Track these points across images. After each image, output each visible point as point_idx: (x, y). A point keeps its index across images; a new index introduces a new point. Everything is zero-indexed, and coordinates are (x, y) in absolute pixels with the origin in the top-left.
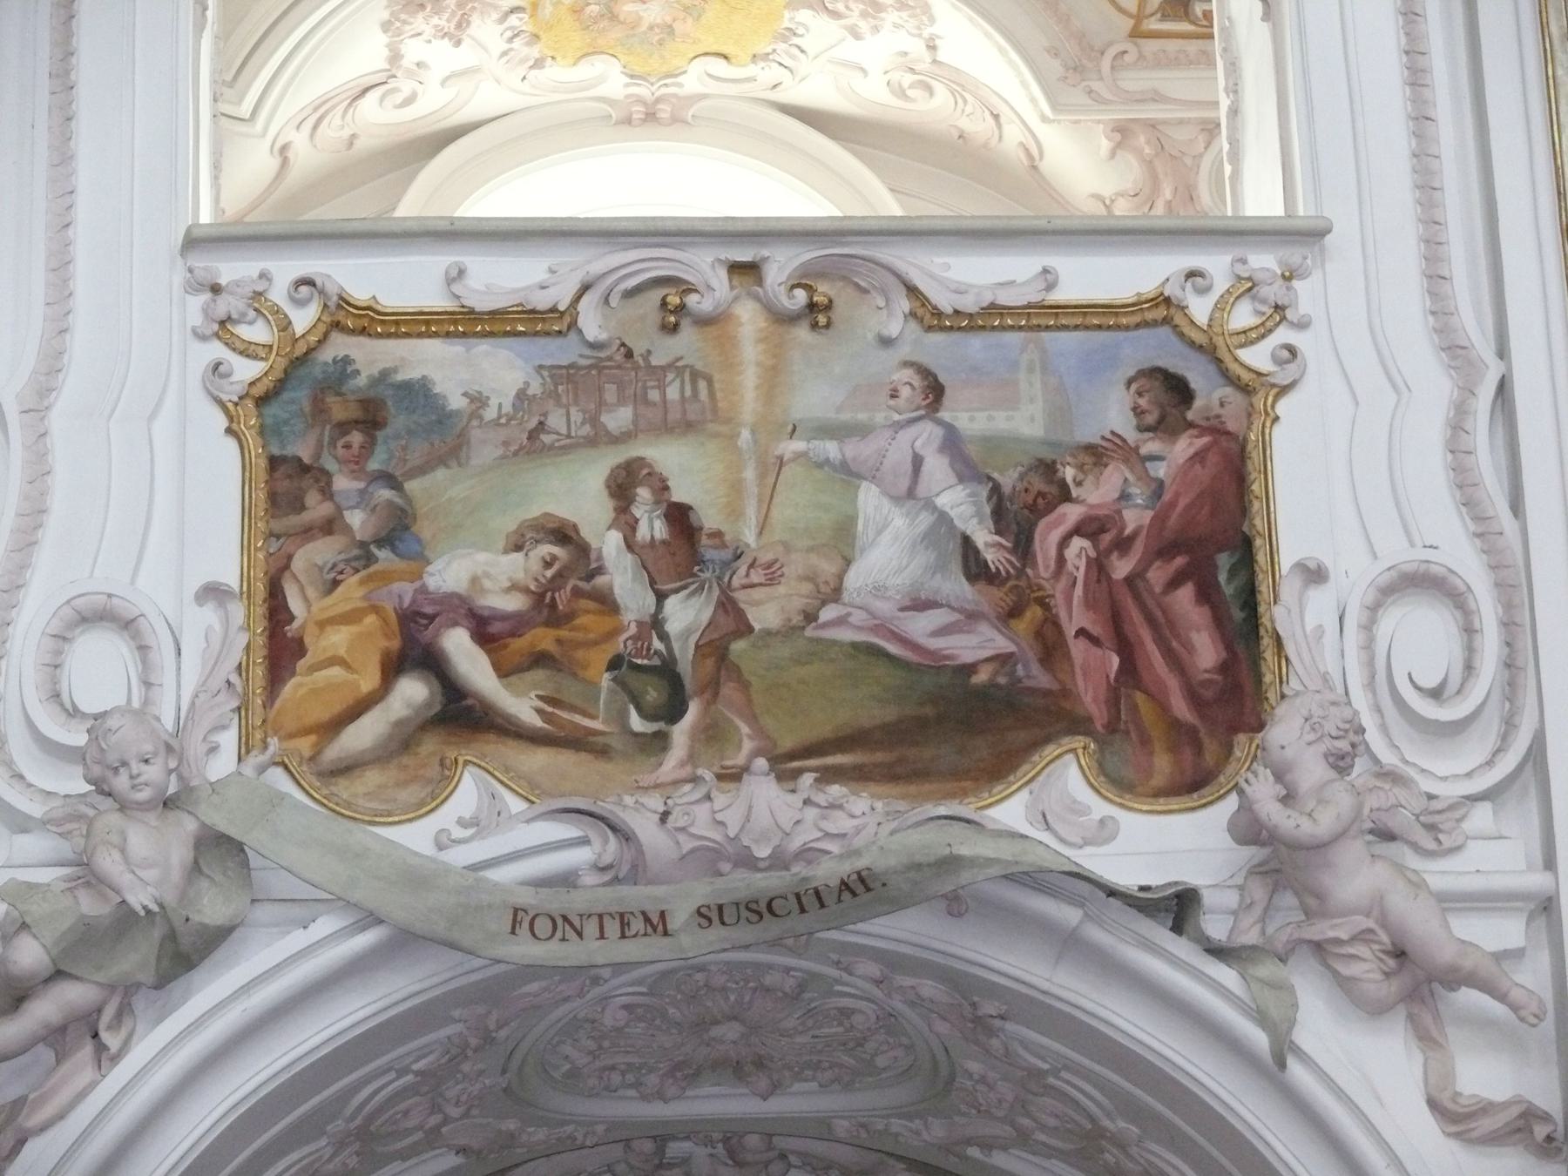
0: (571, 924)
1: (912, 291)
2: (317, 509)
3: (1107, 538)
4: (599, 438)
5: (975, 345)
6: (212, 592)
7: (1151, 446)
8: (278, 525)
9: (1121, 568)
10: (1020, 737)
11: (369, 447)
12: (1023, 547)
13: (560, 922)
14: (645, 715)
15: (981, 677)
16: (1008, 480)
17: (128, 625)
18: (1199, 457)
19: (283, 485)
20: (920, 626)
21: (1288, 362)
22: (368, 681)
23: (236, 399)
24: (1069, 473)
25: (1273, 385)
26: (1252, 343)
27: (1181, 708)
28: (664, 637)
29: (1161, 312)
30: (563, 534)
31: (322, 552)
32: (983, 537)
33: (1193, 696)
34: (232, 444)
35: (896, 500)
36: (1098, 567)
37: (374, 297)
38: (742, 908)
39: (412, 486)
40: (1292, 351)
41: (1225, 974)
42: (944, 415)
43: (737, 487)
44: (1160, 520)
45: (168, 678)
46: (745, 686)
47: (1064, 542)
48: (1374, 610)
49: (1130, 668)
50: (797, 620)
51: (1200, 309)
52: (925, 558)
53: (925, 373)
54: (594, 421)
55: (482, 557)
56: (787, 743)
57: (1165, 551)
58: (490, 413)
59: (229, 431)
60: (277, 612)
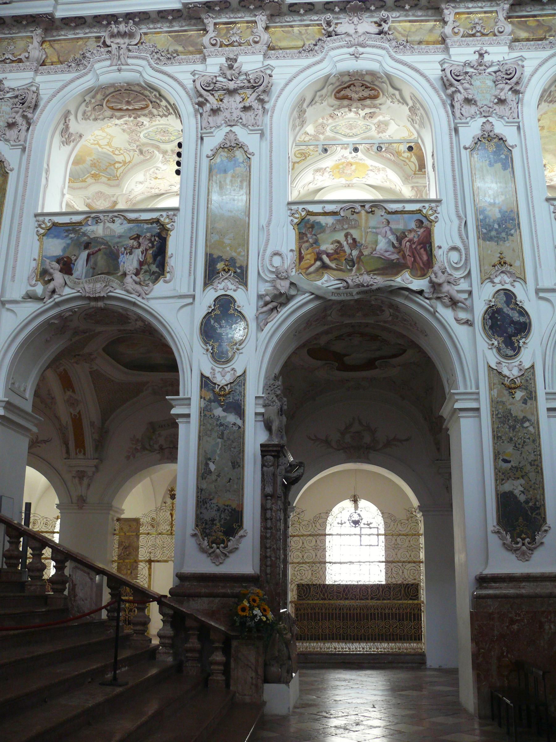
1: (385, 209)
2: (305, 239)
4: (343, 229)
5: (394, 216)
6: (292, 251)
7: (418, 230)
9: (414, 246)
11: (312, 231)
12: (400, 244)
15: (395, 261)
16: (398, 234)
18: (424, 231)
19: (301, 236)
20: (386, 254)
22: (312, 262)
24: (407, 234)
27: (422, 265)
30: (338, 242)
31: (305, 245)
32: (395, 242)
33: (424, 264)
35: (383, 237)
36: (411, 246)
41: (427, 301)
45: (286, 262)
46: (363, 262)
47: (406, 243)
48: (448, 252)
49: (415, 260)
51: (424, 211)
53: (387, 220)
54: (342, 227)
55: (328, 245)
56: (369, 270)
57: (420, 244)
58: (328, 226)
60: (300, 253)
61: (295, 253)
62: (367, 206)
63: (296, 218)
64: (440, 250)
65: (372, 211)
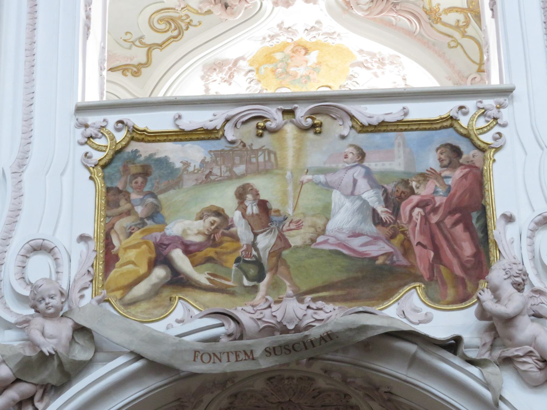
0: (217, 357)
1: (352, 117)
2: (124, 206)
3: (428, 208)
4: (232, 177)
5: (377, 137)
6: (83, 238)
7: (446, 173)
8: (109, 213)
9: (434, 219)
10: (396, 284)
11: (145, 182)
12: (396, 212)
13: (212, 356)
14: (248, 279)
15: (380, 261)
16: (390, 187)
17: (50, 251)
18: (465, 176)
19: (112, 198)
20: (356, 243)
21: (498, 139)
22: (143, 269)
23: (93, 166)
24: (414, 184)
25: (493, 148)
26: (485, 133)
27: (458, 271)
28: (257, 250)
29: (448, 123)
30: (218, 213)
31: (126, 222)
32: (380, 209)
33: (463, 266)
34: (91, 183)
35: (347, 196)
36: (425, 219)
37: (147, 127)
38: (283, 348)
39: (160, 197)
40: (499, 134)
41: (474, 370)
42: (366, 164)
43: (285, 193)
44: (449, 200)
45: (64, 269)
46: (288, 267)
48: (533, 231)
49: (438, 258)
50: (308, 242)
51: (464, 121)
52: (358, 217)
54: (231, 170)
55: (187, 222)
56: (304, 288)
57: (451, 213)
58: (191, 169)
59: (91, 178)
60: (108, 244)
61: (92, 245)
62: (302, 111)
63: (98, 149)
64: (510, 226)
65: (314, 126)
